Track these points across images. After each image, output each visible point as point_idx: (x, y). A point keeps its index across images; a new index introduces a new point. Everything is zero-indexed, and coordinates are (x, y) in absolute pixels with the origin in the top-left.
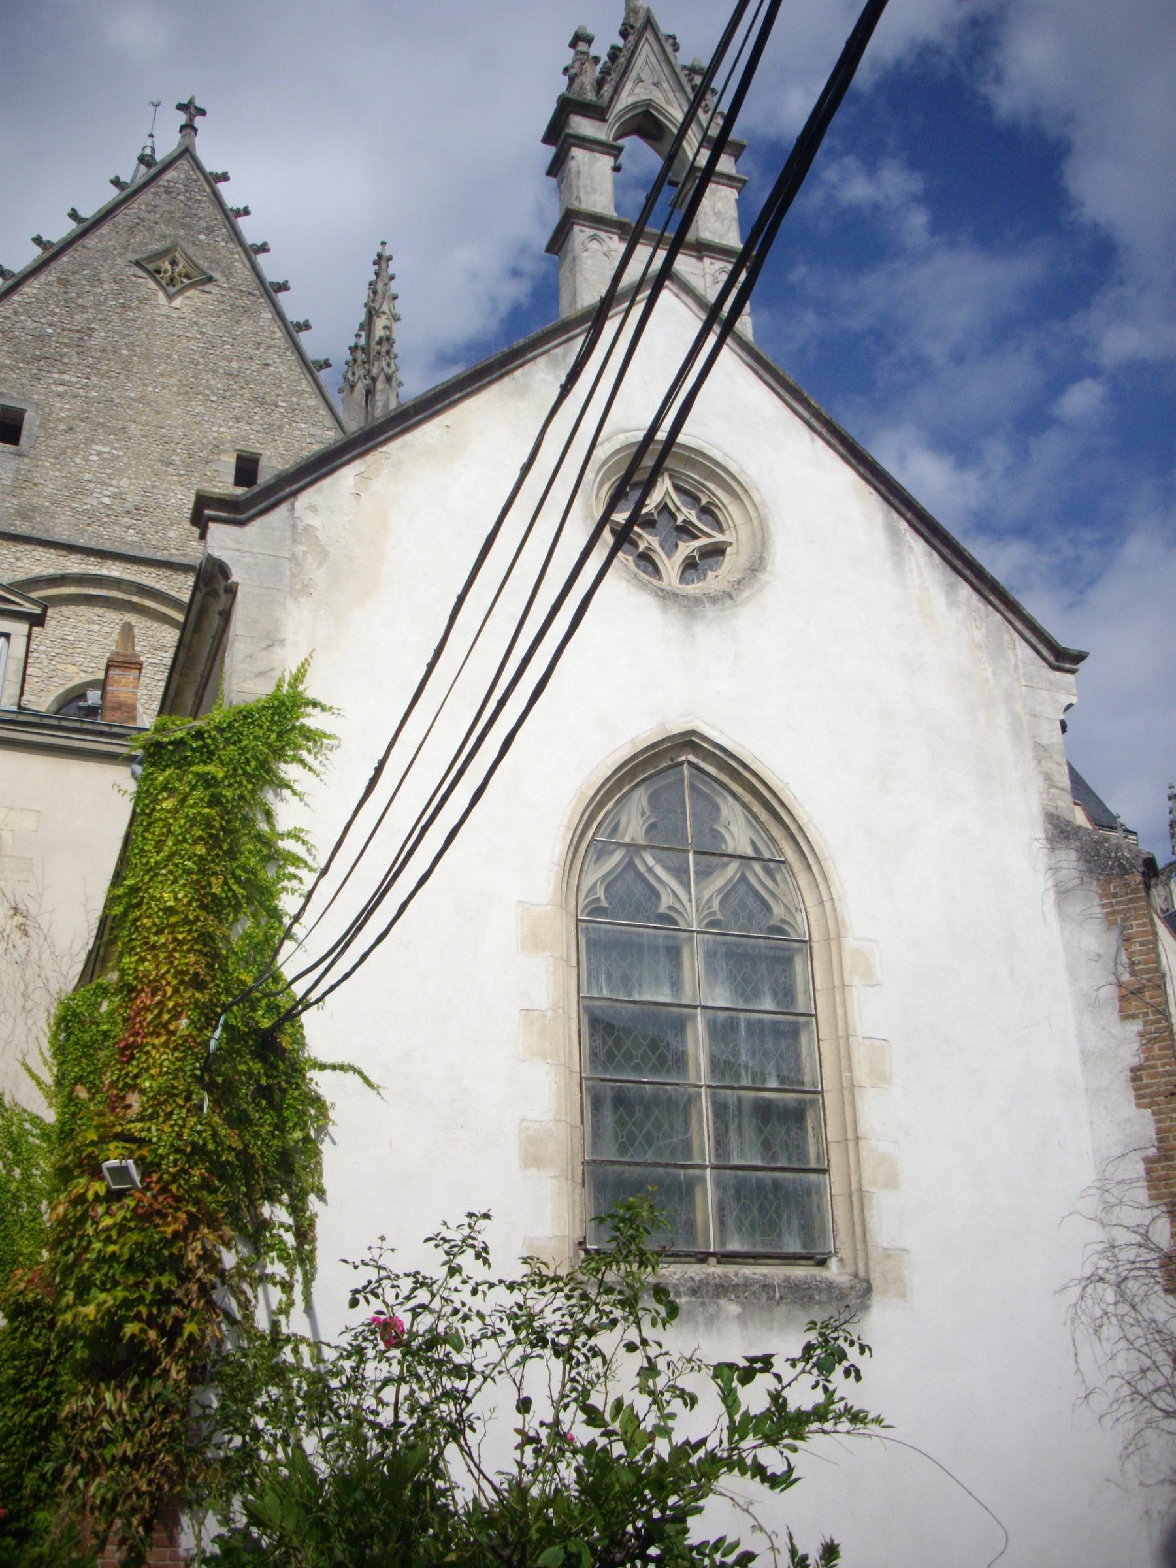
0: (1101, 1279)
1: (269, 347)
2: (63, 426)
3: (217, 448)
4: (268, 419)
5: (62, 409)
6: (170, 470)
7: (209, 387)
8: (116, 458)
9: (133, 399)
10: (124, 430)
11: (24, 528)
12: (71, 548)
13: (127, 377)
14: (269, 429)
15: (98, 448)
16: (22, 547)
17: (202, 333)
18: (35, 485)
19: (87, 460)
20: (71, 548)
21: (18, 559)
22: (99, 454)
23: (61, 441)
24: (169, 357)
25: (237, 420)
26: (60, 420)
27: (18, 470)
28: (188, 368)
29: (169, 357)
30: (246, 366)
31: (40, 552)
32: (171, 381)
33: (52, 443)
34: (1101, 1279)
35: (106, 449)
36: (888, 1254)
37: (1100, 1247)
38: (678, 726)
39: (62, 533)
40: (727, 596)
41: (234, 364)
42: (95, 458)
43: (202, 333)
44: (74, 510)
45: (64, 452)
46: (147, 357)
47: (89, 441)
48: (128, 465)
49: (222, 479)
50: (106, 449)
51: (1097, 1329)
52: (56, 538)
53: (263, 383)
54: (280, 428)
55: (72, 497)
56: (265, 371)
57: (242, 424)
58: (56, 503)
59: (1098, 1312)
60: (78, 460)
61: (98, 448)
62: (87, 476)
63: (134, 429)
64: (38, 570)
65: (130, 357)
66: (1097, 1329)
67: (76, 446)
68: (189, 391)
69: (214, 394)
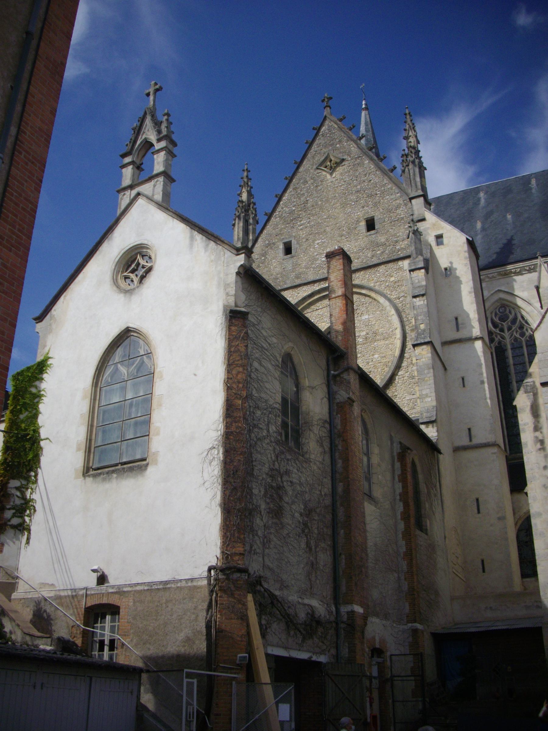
0: (214, 448)
1: (369, 174)
2: (304, 240)
3: (358, 221)
4: (375, 201)
5: (303, 234)
6: (343, 238)
7: (351, 200)
8: (324, 243)
9: (326, 219)
10: (325, 231)
11: (298, 282)
12: (314, 282)
13: (322, 212)
14: (375, 205)
15: (317, 242)
16: (299, 289)
17: (345, 182)
18: (300, 265)
19: (314, 248)
20: (314, 282)
21: (298, 293)
22: (318, 244)
23: (305, 245)
24: (335, 196)
25: (363, 207)
26: (303, 238)
27: (293, 263)
28: (342, 197)
29: (335, 196)
30: (363, 185)
31: (305, 288)
32: (337, 205)
33: (302, 248)
34: (214, 448)
35: (320, 241)
36: (154, 454)
37: (215, 438)
38: (123, 327)
39: (311, 278)
40: (118, 287)
41: (359, 187)
42: (317, 246)
43: (345, 182)
44: (314, 268)
45: (307, 249)
46: (327, 201)
47: (314, 241)
48: (329, 243)
49: (362, 232)
50: (320, 241)
51: (210, 463)
52: (309, 280)
53: (370, 188)
54: (379, 202)
55: (312, 264)
56: (370, 184)
57: (365, 208)
58: (307, 268)
59: (212, 458)
60: (311, 250)
61: (317, 242)
62: (315, 254)
63: (328, 229)
64: (305, 294)
65: (322, 203)
66: (210, 463)
67: (310, 245)
68: (344, 205)
69: (353, 202)
